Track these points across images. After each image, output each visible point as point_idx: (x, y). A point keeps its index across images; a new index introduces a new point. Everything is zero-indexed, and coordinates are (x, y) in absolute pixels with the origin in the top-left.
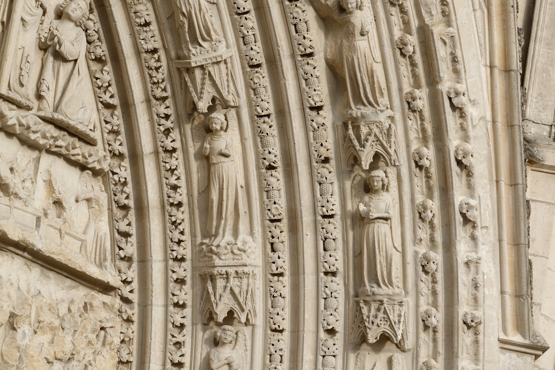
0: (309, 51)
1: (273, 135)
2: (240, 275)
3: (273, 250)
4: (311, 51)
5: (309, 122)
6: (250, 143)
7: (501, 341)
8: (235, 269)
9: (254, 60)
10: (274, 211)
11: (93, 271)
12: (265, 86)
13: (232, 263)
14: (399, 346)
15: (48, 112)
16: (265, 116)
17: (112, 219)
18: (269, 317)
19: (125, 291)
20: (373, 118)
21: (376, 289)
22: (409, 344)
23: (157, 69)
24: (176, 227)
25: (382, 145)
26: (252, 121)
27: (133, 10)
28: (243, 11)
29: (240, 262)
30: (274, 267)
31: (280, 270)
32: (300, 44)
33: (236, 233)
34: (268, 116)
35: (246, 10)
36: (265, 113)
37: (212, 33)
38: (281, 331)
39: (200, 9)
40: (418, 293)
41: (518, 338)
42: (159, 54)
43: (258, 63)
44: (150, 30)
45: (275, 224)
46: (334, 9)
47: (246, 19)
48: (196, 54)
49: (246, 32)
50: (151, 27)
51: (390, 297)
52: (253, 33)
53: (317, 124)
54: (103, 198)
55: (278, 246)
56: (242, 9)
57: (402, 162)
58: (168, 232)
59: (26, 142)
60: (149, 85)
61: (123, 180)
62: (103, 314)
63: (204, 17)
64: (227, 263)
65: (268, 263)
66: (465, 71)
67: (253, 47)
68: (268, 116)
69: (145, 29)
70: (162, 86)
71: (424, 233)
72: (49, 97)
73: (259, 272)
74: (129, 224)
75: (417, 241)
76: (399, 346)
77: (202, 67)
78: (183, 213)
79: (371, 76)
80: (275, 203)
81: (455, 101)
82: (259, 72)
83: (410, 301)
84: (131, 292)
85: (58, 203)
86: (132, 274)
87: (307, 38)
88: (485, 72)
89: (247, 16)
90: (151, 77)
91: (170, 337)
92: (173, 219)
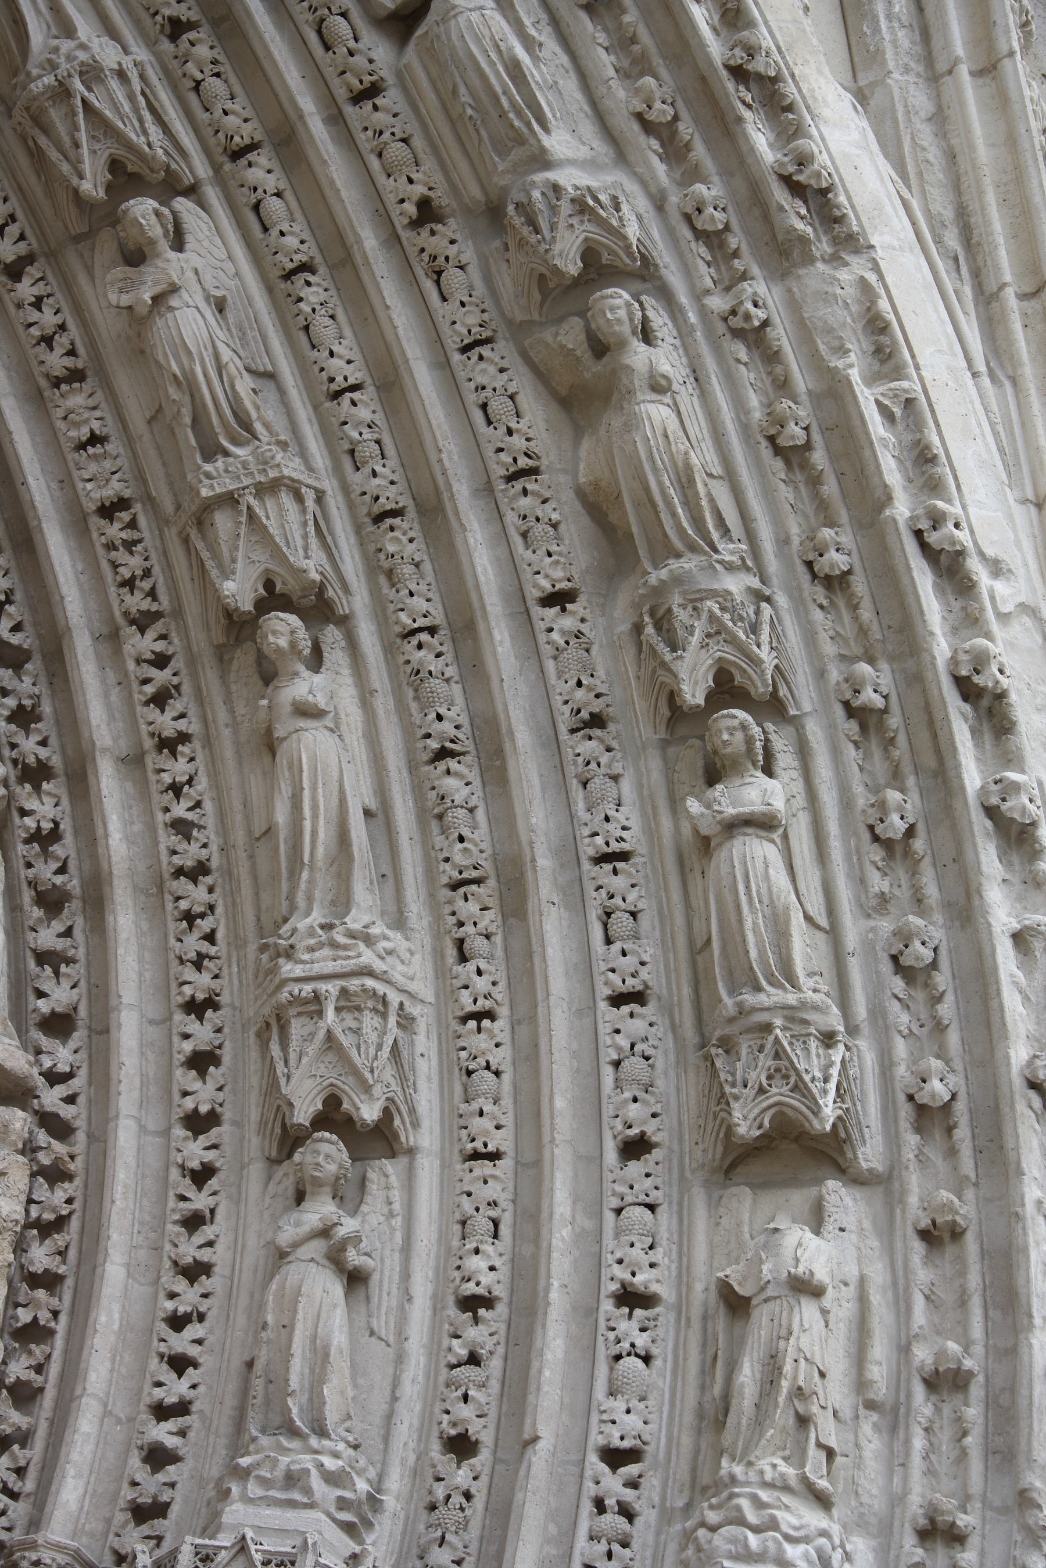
0: (523, 462)
1: (447, 675)
2: (357, 1001)
3: (463, 958)
4: (530, 463)
5: (542, 638)
6: (384, 704)
8: (340, 983)
9: (382, 500)
10: (459, 859)
12: (417, 559)
13: (329, 967)
16: (420, 630)
19: (51, 1098)
20: (705, 583)
21: (749, 998)
23: (129, 545)
24: (191, 926)
25: (733, 641)
26: (389, 650)
27: (60, 413)
28: (345, 385)
29: (350, 964)
30: (466, 997)
31: (483, 1004)
32: (501, 450)
33: (342, 903)
34: (432, 630)
35: (351, 381)
36: (421, 622)
38: (494, 1157)
39: (220, 368)
42: (132, 511)
43: (394, 506)
44: (105, 455)
45: (462, 890)
46: (578, 353)
47: (354, 403)
48: (215, 474)
49: (355, 435)
50: (109, 447)
51: (794, 1015)
52: (376, 436)
53: (563, 632)
55: (478, 944)
56: (339, 379)
57: (807, 707)
58: (172, 941)
60: (112, 590)
61: (47, 826)
63: (232, 386)
64: (317, 969)
66: (958, 487)
67: (378, 469)
68: (432, 630)
69: (91, 450)
70: (146, 585)
74: (68, 933)
77: (230, 500)
78: (211, 890)
79: (686, 481)
80: (461, 839)
81: (933, 538)
82: (399, 527)
84: (71, 1100)
87: (518, 431)
89: (356, 395)
90: (115, 566)
91: (172, 1202)
92: (184, 905)
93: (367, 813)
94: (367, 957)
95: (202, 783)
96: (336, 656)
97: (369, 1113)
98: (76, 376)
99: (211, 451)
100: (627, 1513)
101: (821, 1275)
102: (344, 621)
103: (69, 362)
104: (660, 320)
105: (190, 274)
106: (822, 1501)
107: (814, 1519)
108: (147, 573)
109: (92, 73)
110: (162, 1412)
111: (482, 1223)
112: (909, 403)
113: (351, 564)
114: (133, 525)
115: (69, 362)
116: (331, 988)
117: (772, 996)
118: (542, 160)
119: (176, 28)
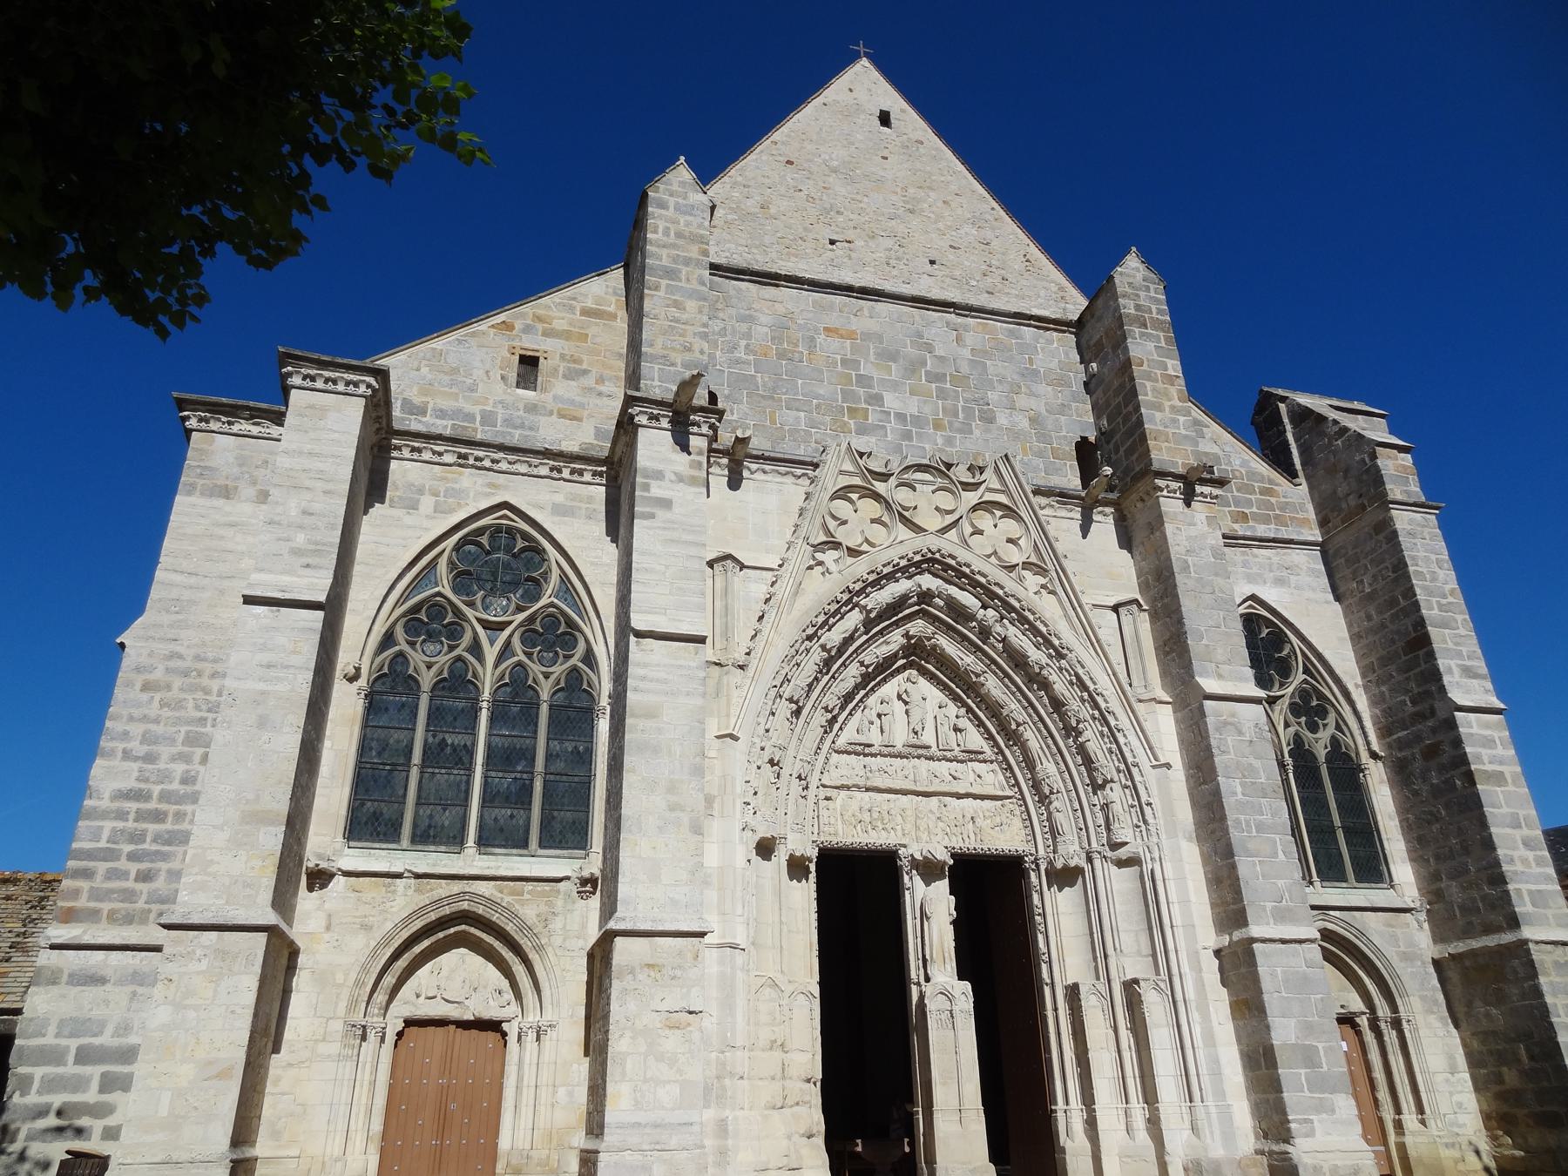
11: (1000, 793)
14: (1112, 781)
15: (963, 748)
17: (1004, 774)
18: (1065, 787)
22: (1116, 779)
40: (1113, 761)
41: (1155, 763)
54: (998, 768)
59: (962, 762)
62: (1011, 806)
65: (1058, 769)
71: (1106, 740)
72: (962, 744)
73: (1057, 774)
75: (1105, 743)
76: (1112, 781)
85: (979, 776)
86: (1016, 790)
88: (1107, 678)
104: (1051, 671)
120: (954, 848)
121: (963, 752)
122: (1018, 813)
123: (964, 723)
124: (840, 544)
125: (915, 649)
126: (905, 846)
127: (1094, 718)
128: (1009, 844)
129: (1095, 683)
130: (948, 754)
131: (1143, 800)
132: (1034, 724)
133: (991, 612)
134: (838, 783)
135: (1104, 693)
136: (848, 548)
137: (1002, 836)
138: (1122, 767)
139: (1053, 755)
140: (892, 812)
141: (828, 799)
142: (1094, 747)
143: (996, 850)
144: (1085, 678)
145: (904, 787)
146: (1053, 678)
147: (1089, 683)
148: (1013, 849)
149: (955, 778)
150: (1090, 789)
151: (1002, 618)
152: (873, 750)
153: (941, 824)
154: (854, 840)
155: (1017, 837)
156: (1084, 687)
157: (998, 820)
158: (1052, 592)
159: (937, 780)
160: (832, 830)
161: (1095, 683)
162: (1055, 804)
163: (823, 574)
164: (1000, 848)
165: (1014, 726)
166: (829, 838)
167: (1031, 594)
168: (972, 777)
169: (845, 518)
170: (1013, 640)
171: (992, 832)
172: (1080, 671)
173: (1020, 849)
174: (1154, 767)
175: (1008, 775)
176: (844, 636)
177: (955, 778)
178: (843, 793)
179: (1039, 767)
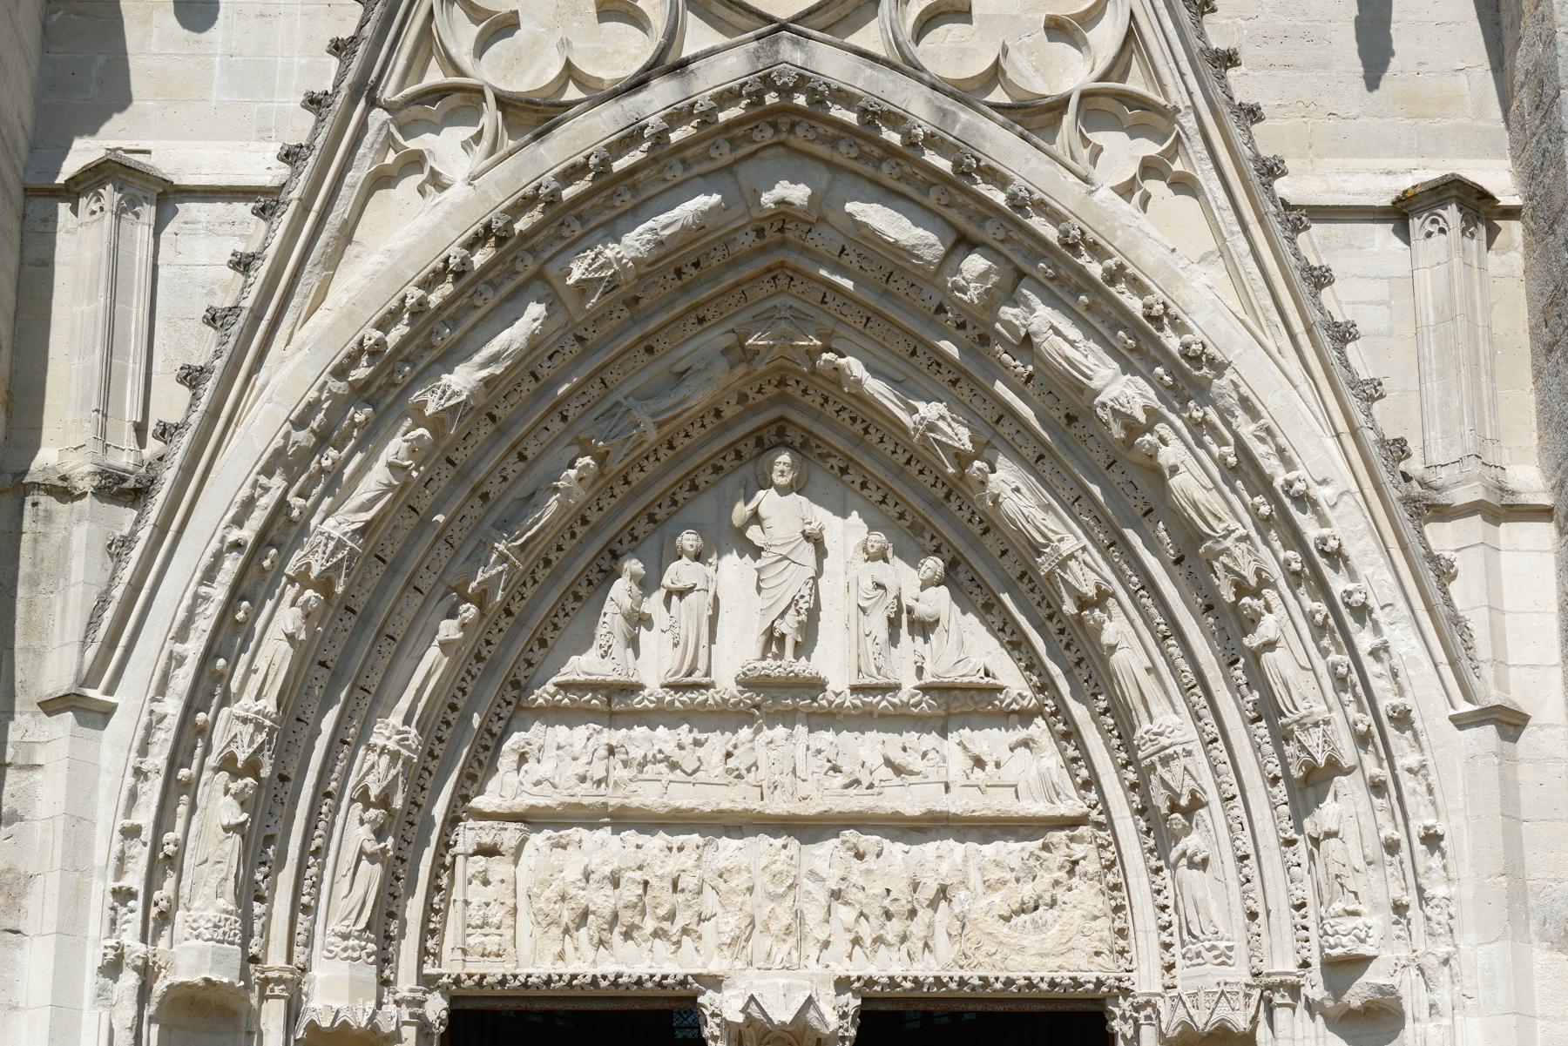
7: (1453, 719)
17: (1062, 751)
31: (1212, 736)
37: (1050, 534)
41: (1465, 707)
57: (1276, 576)
65: (1201, 731)
73: (1197, 747)
75: (1324, 653)
83: (1337, 716)
88: (1331, 443)
93: (1148, 670)
94: (1164, 741)
95: (1094, 674)
96: (1116, 610)
97: (1184, 802)
98: (986, 531)
99: (1040, 554)
100: (1306, 928)
101: (1334, 828)
102: (1113, 595)
103: (981, 526)
105: (1002, 484)
106: (1355, 914)
107: (1351, 922)
108: (1043, 598)
109: (932, 427)
110: (1164, 928)
111: (1236, 826)
112: (1268, 430)
113: (1107, 572)
114: (1031, 580)
115: (981, 526)
116: (1155, 758)
117: (1291, 718)
118: (1096, 393)
119: (954, 383)
120: (871, 982)
121: (925, 689)
122: (1091, 866)
123: (938, 601)
124: (479, 91)
125: (782, 382)
126: (715, 982)
127: (1294, 578)
128: (1053, 962)
129: (1288, 464)
130: (882, 703)
131: (1416, 828)
132: (1133, 596)
133: (975, 263)
134: (522, 803)
135: (1322, 494)
136: (504, 102)
137: (1030, 940)
138: (1365, 721)
139: (1186, 691)
140: (687, 882)
141: (489, 851)
142: (1290, 671)
143: (1009, 982)
144: (1259, 449)
145: (726, 805)
146: (1171, 453)
147: (1271, 465)
148: (1063, 977)
149: (899, 770)
150: (1281, 791)
151: (1021, 275)
152: (637, 702)
153: (845, 914)
154: (567, 969)
155: (1079, 941)
156: (1261, 483)
157: (1027, 891)
158: (1184, 185)
159: (840, 780)
160: (492, 943)
161: (1288, 464)
162: (1192, 842)
163: (421, 191)
164: (1019, 976)
165: (1069, 607)
166: (477, 967)
167: (1104, 195)
168: (958, 763)
169: (504, 8)
170: (1051, 345)
171: (1003, 929)
172: (1247, 429)
173: (1088, 977)
174: (1461, 722)
175: (1071, 752)
176: (484, 373)
177: (899, 770)
178: (539, 840)
179: (1143, 728)
